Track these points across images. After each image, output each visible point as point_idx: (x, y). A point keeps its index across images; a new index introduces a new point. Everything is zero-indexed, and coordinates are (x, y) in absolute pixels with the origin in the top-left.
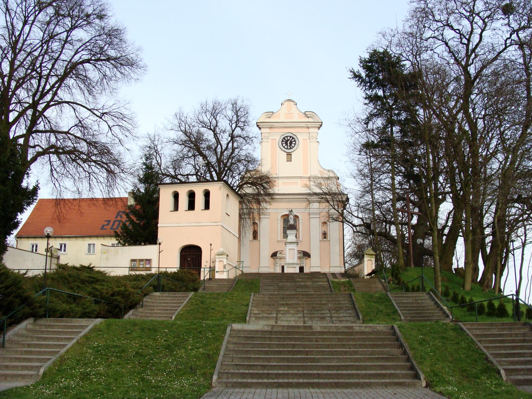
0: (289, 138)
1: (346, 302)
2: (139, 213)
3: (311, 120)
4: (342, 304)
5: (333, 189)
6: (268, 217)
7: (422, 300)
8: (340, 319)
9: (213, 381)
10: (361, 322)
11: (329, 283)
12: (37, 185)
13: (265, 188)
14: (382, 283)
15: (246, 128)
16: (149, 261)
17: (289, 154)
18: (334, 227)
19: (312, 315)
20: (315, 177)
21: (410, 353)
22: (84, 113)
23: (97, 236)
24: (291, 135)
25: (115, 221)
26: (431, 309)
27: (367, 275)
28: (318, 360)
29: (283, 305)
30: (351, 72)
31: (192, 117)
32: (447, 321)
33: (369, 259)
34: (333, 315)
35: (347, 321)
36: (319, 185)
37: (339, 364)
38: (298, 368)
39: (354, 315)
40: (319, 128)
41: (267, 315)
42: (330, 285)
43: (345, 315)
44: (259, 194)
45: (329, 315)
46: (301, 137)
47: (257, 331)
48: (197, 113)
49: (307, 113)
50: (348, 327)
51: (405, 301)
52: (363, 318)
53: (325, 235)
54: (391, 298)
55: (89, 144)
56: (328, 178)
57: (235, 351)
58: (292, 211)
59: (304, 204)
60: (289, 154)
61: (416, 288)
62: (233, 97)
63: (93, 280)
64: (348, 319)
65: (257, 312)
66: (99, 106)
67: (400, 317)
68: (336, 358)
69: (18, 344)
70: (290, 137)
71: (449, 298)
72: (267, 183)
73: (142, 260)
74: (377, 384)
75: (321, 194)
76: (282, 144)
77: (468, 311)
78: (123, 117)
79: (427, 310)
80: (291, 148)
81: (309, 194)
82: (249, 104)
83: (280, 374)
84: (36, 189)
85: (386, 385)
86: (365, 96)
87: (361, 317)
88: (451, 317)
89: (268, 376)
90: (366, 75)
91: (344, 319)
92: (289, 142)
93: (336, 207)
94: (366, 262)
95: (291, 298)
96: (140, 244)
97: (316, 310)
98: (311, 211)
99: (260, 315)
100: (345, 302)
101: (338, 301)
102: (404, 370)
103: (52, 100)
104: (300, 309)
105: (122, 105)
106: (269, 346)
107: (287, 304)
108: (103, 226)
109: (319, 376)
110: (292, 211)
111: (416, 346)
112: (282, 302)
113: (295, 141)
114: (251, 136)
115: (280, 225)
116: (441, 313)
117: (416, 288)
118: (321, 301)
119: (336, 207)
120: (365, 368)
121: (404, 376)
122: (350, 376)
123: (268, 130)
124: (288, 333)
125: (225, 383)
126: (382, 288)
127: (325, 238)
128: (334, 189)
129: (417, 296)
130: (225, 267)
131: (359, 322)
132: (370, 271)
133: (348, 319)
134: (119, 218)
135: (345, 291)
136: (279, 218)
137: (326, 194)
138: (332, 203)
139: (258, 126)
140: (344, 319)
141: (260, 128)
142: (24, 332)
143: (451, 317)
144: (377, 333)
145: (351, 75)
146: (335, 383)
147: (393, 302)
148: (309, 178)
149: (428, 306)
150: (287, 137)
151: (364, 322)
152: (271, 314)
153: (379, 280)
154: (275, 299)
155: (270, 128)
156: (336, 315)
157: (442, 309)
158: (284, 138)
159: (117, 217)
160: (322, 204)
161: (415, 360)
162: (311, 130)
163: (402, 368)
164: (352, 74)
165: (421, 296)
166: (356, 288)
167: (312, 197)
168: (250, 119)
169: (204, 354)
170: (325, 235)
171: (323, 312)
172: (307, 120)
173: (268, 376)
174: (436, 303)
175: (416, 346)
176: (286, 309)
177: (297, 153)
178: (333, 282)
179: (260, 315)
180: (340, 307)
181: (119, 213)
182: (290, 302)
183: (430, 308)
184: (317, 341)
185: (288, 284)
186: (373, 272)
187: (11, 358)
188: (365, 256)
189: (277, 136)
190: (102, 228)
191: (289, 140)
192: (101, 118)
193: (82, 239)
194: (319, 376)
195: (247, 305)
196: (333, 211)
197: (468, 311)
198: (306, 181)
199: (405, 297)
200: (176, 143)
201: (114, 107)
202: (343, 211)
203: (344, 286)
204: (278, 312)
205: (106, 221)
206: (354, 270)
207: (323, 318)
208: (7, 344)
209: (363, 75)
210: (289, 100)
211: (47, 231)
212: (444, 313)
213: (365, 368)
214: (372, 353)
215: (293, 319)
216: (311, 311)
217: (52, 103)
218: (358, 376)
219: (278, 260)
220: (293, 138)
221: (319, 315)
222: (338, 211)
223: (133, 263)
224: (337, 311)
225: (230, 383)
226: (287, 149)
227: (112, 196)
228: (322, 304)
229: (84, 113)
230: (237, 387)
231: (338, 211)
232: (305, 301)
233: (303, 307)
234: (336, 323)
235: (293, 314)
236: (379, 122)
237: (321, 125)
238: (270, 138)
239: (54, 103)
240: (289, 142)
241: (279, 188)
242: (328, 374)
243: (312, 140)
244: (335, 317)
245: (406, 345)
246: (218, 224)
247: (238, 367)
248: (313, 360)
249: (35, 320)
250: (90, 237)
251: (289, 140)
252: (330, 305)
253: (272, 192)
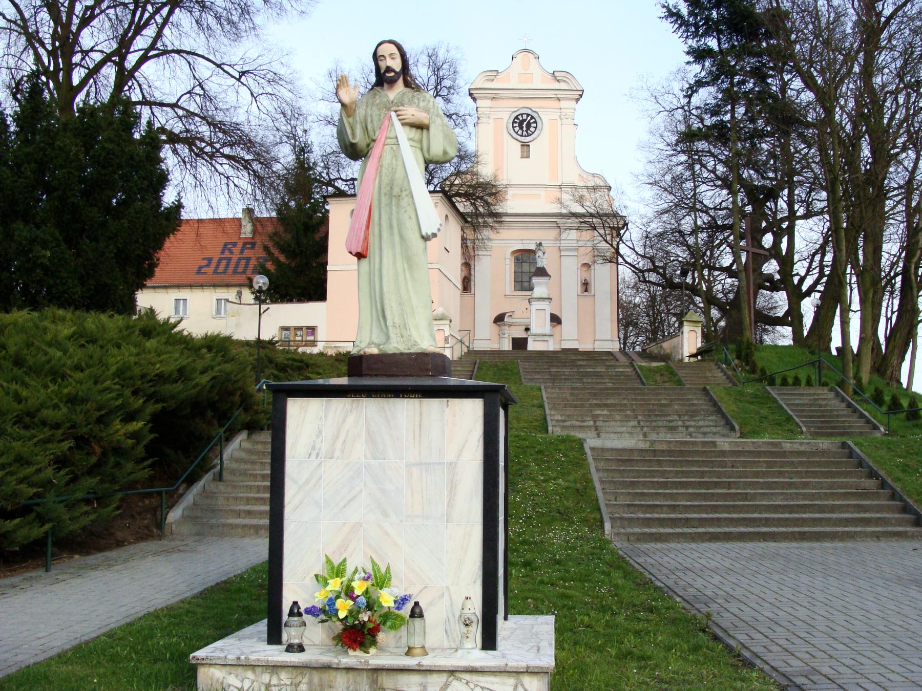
0: (525, 117)
1: (700, 402)
2: (289, 246)
3: (563, 86)
4: (696, 405)
5: (605, 206)
6: (489, 253)
7: (825, 399)
8: (702, 430)
9: (607, 532)
10: (738, 435)
11: (635, 369)
12: (179, 201)
13: (488, 204)
14: (722, 371)
15: (455, 98)
16: (312, 330)
17: (525, 146)
18: (602, 274)
19: (654, 424)
20: (576, 187)
21: (898, 487)
22: (204, 69)
23: (191, 286)
24: (529, 112)
25: (221, 260)
26: (845, 416)
27: (690, 356)
28: (753, 497)
29: (599, 406)
30: (664, 7)
31: (359, 77)
32: (878, 435)
33: (692, 328)
34: (688, 424)
35: (715, 433)
36: (580, 200)
37: (786, 503)
38: (728, 509)
39: (722, 422)
40: (577, 100)
41: (578, 424)
42: (637, 372)
43: (707, 423)
44: (477, 215)
45: (680, 423)
46: (546, 115)
47: (631, 451)
48: (367, 70)
49: (556, 74)
50: (772, 444)
51: (797, 402)
52: (741, 428)
53: (586, 286)
54: (775, 396)
55: (212, 123)
56: (595, 188)
57: (614, 482)
58: (540, 244)
59: (553, 233)
60: (525, 146)
61: (790, 381)
62: (431, 43)
63: (299, 364)
64: (714, 430)
65: (559, 418)
66: (235, 59)
67: (800, 427)
68: (782, 494)
69: (245, 474)
70: (528, 115)
71: (867, 395)
72: (491, 195)
73: (300, 328)
74: (866, 535)
75: (583, 215)
76: (513, 127)
77: (908, 419)
78: (277, 79)
79: (838, 416)
81: (561, 215)
82: (458, 56)
83: (705, 519)
84: (178, 206)
85: (877, 536)
86: (686, 50)
87: (737, 427)
88: (882, 429)
89: (687, 522)
90: (691, 14)
91: (708, 430)
92: (525, 124)
93: (609, 238)
94: (686, 335)
95: (607, 394)
96: (290, 301)
97: (657, 416)
98: (563, 244)
99: (568, 424)
100: (700, 402)
101: (688, 400)
102: (893, 512)
103: (153, 46)
104: (628, 412)
105: (275, 58)
106: (663, 474)
107: (606, 405)
108: (201, 268)
109: (767, 522)
110: (540, 244)
111: (901, 475)
112: (595, 402)
113: (535, 122)
114: (461, 114)
115: (508, 269)
116: (861, 423)
117: (790, 381)
118: (659, 400)
119: (609, 238)
120: (833, 509)
121: (899, 523)
122: (815, 522)
123: (488, 103)
124: (681, 453)
125: (625, 534)
126: (724, 378)
127: (586, 291)
128: (606, 208)
129: (814, 394)
130: (446, 340)
131: (733, 434)
132: (695, 351)
133: (714, 430)
134: (227, 254)
135: (664, 382)
136: (508, 255)
137: (592, 215)
138: (602, 232)
139: (471, 95)
140: (708, 430)
141: (474, 99)
142: (243, 455)
143: (882, 429)
144: (823, 453)
145: (662, 12)
146: (800, 533)
147: (781, 402)
148: (560, 187)
149: (837, 411)
150: (522, 115)
151: (742, 435)
152: (583, 421)
153: (716, 364)
154: (581, 396)
155: (493, 98)
156: (693, 423)
157: (862, 416)
158: (517, 117)
159: (223, 253)
160: (584, 233)
161: (911, 498)
162: (564, 104)
163: (889, 509)
164: (665, 10)
165: (819, 394)
166: (683, 379)
167: (569, 221)
168: (460, 82)
169: (567, 488)
170: (586, 286)
171: (669, 418)
172: (557, 86)
173: (687, 522)
174: (849, 405)
175: (901, 475)
176: (605, 412)
177: (539, 143)
178: (640, 367)
179: (568, 424)
180: (695, 411)
181: (226, 244)
182: (609, 402)
183: (841, 413)
184: (733, 467)
185: (567, 371)
186: (700, 352)
187: (248, 499)
188: (685, 323)
189: (505, 113)
190: (199, 272)
191: (525, 120)
192: (239, 80)
193: (163, 291)
194: (767, 522)
195: (542, 406)
196: (604, 245)
197: (908, 419)
198: (555, 193)
199: (795, 394)
200: (329, 123)
201: (260, 61)
202: (618, 244)
203: (662, 375)
204: (595, 418)
205: (204, 259)
206: (661, 347)
207: (673, 429)
208: (226, 475)
209: (684, 11)
210: (526, 51)
211: (258, 283)
212: (868, 421)
213: (833, 509)
214: (831, 486)
215: (624, 429)
216: (649, 416)
217: (151, 54)
218: (828, 522)
219: (506, 328)
220: (532, 117)
221: (665, 424)
222: (612, 245)
223: (284, 332)
224: (691, 416)
225: (634, 534)
226: (522, 136)
227: (216, 217)
228: (663, 405)
229: (204, 69)
230: (646, 541)
231: (612, 245)
232: (633, 400)
233: (634, 410)
234: (696, 437)
235: (622, 421)
236: (706, 96)
237: (581, 96)
238: (493, 117)
239: (157, 52)
240: (525, 124)
241: (511, 204)
242: (782, 519)
243: (565, 121)
244: (693, 427)
245: (882, 473)
246: (434, 266)
247: (632, 509)
248: (745, 497)
249: (249, 435)
250: (179, 286)
251: (525, 120)
252: (676, 407)
253: (500, 211)
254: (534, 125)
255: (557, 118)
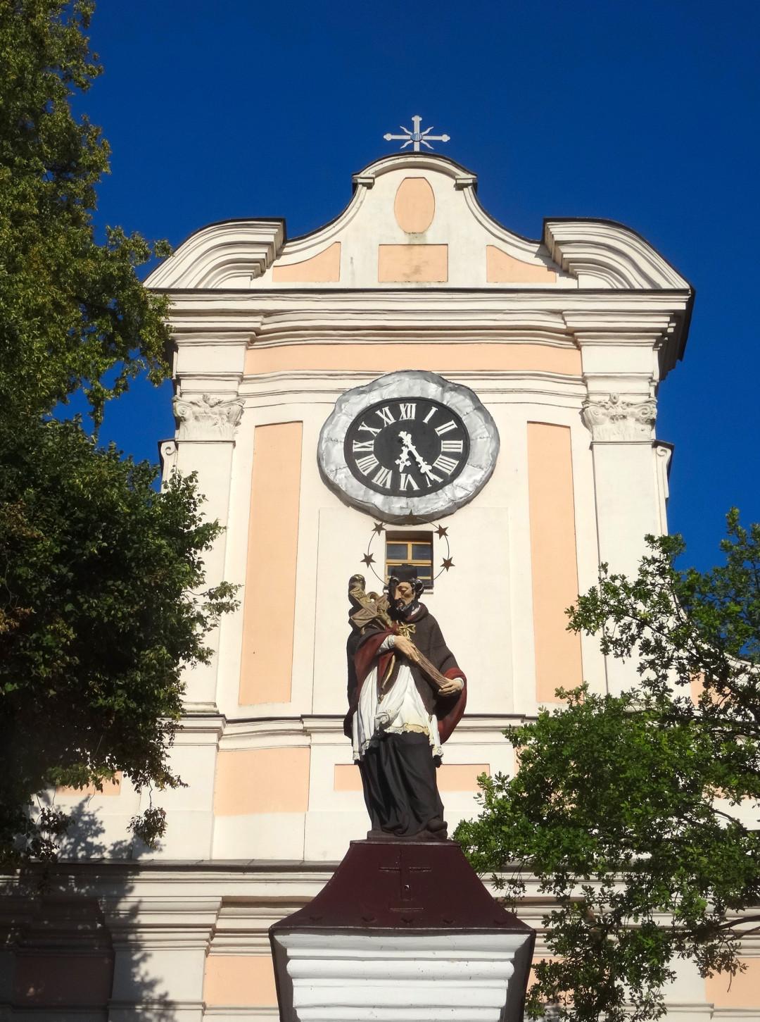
24: (433, 391)
70: (423, 404)
76: (351, 458)
80: (426, 488)
113: (461, 433)
123: (232, 357)
150: (394, 404)
155: (255, 338)
158: (368, 415)
162: (596, 357)
220: (446, 413)
226: (394, 491)
243: (606, 430)
254: (456, 446)
255: (574, 420)
